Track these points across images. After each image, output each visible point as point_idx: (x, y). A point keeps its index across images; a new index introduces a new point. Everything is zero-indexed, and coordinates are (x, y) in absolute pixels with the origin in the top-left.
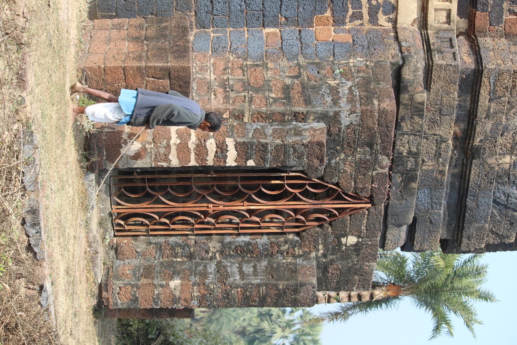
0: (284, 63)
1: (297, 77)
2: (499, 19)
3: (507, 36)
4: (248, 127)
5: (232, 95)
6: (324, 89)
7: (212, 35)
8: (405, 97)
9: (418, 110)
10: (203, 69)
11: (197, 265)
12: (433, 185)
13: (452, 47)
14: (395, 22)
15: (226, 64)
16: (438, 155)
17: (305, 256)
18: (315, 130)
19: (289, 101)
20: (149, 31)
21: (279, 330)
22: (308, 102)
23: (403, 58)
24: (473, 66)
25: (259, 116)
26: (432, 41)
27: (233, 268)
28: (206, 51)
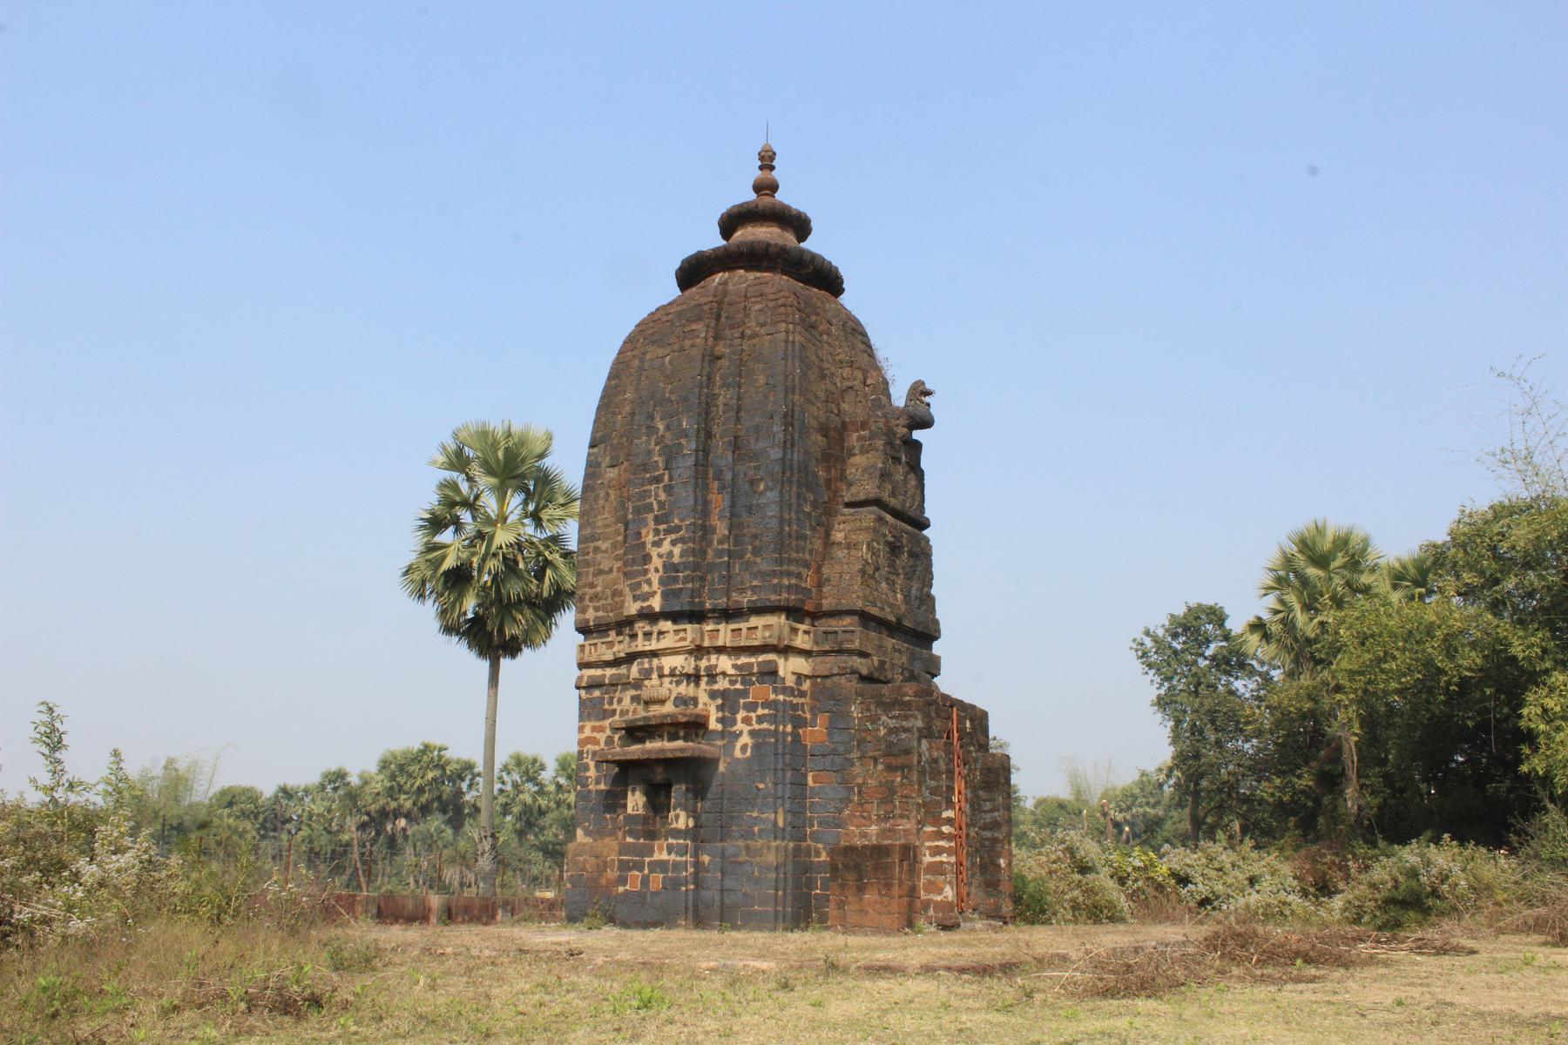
0: (857, 769)
1: (875, 760)
2: (809, 591)
3: (820, 585)
5: (898, 812)
6: (893, 738)
8: (876, 675)
9: (882, 663)
10: (864, 835)
11: (982, 845)
12: (912, 657)
16: (900, 651)
17: (976, 760)
21: (521, 796)
22: (907, 752)
23: (853, 672)
25: (920, 790)
27: (988, 818)
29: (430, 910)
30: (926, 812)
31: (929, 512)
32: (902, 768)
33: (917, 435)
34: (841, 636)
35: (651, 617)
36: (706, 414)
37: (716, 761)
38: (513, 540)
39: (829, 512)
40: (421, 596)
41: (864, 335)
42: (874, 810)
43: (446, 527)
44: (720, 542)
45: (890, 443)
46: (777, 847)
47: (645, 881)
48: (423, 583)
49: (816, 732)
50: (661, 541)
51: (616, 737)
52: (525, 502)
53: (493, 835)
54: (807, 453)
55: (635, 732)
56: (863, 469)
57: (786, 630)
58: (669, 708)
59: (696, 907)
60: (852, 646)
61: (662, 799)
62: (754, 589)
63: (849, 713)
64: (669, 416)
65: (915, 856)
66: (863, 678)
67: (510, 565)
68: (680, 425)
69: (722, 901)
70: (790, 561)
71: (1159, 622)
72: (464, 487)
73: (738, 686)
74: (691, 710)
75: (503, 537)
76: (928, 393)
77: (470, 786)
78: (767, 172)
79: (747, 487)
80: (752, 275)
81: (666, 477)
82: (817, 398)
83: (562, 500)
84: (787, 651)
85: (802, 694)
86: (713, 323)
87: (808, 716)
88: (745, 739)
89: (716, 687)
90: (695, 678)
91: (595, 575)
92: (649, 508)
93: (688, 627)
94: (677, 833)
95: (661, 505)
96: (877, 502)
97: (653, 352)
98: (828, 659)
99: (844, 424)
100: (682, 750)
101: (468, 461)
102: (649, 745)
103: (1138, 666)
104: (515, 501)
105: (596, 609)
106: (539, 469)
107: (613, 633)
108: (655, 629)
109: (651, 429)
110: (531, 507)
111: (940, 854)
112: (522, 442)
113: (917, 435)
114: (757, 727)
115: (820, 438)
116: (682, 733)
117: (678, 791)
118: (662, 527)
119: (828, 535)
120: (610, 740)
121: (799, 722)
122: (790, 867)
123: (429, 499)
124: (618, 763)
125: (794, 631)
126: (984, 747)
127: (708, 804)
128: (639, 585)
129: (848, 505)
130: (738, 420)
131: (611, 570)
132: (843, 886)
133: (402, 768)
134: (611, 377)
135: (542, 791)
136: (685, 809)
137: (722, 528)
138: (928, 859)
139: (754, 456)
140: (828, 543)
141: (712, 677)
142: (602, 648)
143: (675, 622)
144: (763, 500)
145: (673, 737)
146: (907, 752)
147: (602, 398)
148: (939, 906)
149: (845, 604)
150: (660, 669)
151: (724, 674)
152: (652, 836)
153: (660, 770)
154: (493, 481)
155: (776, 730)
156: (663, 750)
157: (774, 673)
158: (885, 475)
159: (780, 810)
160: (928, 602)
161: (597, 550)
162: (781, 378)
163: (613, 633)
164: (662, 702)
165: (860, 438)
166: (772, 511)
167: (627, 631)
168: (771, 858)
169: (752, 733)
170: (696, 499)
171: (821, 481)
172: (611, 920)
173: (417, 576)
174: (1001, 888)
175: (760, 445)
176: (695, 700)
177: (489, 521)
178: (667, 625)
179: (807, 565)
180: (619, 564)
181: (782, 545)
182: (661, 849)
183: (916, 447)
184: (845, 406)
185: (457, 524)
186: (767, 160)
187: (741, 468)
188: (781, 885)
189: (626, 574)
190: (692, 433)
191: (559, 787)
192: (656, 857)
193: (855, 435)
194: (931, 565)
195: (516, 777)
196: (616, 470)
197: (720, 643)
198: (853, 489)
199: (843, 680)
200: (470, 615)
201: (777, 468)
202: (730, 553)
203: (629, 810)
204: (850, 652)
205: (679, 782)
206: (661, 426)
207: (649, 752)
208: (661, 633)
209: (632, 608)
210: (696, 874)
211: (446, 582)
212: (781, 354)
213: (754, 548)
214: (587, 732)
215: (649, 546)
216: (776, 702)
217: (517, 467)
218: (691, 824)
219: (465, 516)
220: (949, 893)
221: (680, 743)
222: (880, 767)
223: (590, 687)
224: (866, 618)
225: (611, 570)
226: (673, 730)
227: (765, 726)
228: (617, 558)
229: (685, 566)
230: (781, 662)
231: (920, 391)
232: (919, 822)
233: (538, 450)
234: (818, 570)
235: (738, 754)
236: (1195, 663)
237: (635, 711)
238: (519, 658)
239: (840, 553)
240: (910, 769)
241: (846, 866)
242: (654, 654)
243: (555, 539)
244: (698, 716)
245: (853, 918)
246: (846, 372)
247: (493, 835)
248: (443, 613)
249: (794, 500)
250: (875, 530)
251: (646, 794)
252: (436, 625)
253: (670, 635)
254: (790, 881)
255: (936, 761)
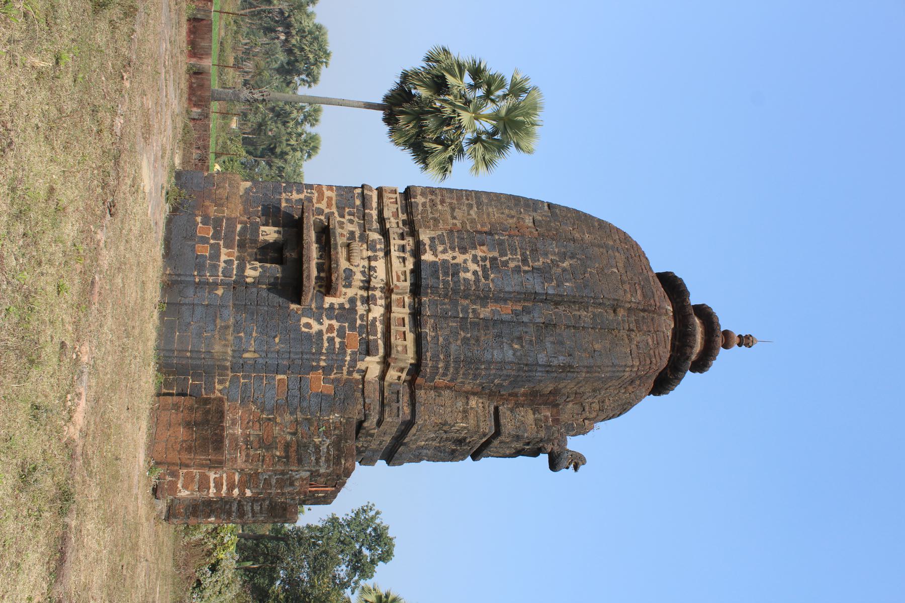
0: (288, 417)
1: (294, 434)
3: (436, 388)
4: (261, 477)
5: (252, 452)
6: (312, 449)
7: (242, 381)
9: (372, 435)
10: (234, 423)
12: (374, 451)
13: (398, 402)
14: (364, 377)
15: (249, 416)
16: (380, 444)
18: (302, 479)
19: (288, 461)
20: (198, 415)
22: (300, 461)
23: (365, 415)
24: (409, 418)
26: (386, 394)
27: (248, 508)
28: (237, 401)
29: (201, 58)
30: (251, 475)
31: (486, 462)
32: (287, 457)
33: (544, 458)
34: (395, 405)
35: (417, 252)
36: (573, 301)
37: (299, 303)
38: (463, 124)
39: (491, 395)
40: (428, 59)
41: (619, 416)
42: (254, 432)
43: (474, 79)
44: (474, 311)
45: (541, 440)
46: (226, 353)
47: (204, 240)
48: (437, 61)
49: (319, 383)
50: (477, 263)
51: (322, 218)
52: (487, 133)
53: (264, 100)
54: (540, 381)
55: (325, 234)
56: (523, 420)
57: (402, 365)
58: (344, 264)
59: (181, 282)
60: (386, 416)
61: (271, 254)
62: (436, 338)
63: (333, 411)
64: (573, 271)
65: (215, 467)
66: (360, 424)
67: (448, 121)
68: (567, 281)
69: (186, 304)
70: (457, 370)
71: (383, 520)
72: (500, 93)
73: (359, 322)
74: (341, 283)
75: (465, 117)
76: (576, 468)
77: (303, 80)
78: (737, 340)
79: (517, 334)
80: (670, 334)
81: (526, 268)
82: (579, 388)
83: (487, 157)
84: (386, 364)
85: (350, 373)
86: (641, 307)
87: (332, 376)
88: (316, 327)
89: (359, 303)
90: (367, 285)
91: (450, 204)
92: (503, 254)
93: (408, 284)
94: (241, 268)
95: (505, 264)
96: (498, 433)
97: (620, 258)
98: (377, 394)
99: (558, 405)
100: (309, 276)
101: (517, 96)
102: (314, 247)
103: (357, 507)
104: (488, 126)
105: (424, 205)
106: (508, 143)
107: (404, 217)
108: (407, 255)
109: (563, 256)
110: (484, 137)
111: (216, 487)
112: (528, 134)
113: (544, 458)
114: (325, 337)
115: (550, 389)
116: (322, 275)
117: (276, 270)
118: (488, 263)
119: (474, 394)
120: (320, 212)
121: (327, 370)
122: (210, 362)
123: (492, 68)
124: (301, 219)
125: (401, 370)
126: (303, 502)
127: (264, 294)
128: (443, 243)
129: (496, 409)
130: (568, 327)
131: (454, 218)
132: (191, 409)
133: (316, 38)
134: (601, 223)
135: (298, 124)
136: (260, 276)
137: (485, 312)
138: (212, 476)
139: (540, 340)
140: (467, 395)
141: (367, 300)
142: (393, 208)
143: (412, 271)
144: (506, 347)
145: (320, 268)
146: (300, 461)
147: (585, 215)
148: (173, 487)
149: (420, 409)
150: (375, 258)
151: (369, 310)
152: (242, 246)
153: (294, 255)
154: (503, 112)
155: (321, 354)
156: (309, 261)
157: (368, 353)
158: (518, 438)
159: (256, 355)
160: (418, 458)
161: (470, 206)
162: (599, 363)
163: (404, 217)
164: (349, 259)
165: (546, 417)
166: (497, 355)
167: (406, 229)
168: (217, 348)
169: (320, 333)
170: (510, 293)
171: (516, 390)
172: (175, 210)
173: (442, 57)
174: (191, 518)
175: (548, 345)
176: (349, 286)
177: (477, 108)
178: (410, 265)
179: (452, 380)
180: (459, 225)
181: (470, 363)
182: (229, 255)
183: (535, 453)
184: (570, 405)
185: (473, 87)
186: (745, 341)
187: (531, 329)
188: (195, 355)
189: (451, 231)
190: (561, 291)
191: (300, 135)
192: (224, 251)
193: (549, 414)
194: (443, 460)
195: (307, 109)
196: (531, 224)
197: (394, 308)
198: (509, 412)
199: (360, 407)
200: (413, 91)
201: (531, 360)
202: (464, 319)
203: (262, 228)
204: (382, 413)
205: (283, 271)
206: (565, 264)
207: (309, 249)
208: (404, 259)
209: (425, 236)
210: (208, 283)
211: (437, 77)
212: (616, 362)
213: (468, 339)
214: (328, 193)
215: (473, 252)
216: (345, 352)
217: (511, 129)
218: (249, 280)
219: (480, 92)
220: (184, 493)
221: (314, 273)
222: (289, 438)
223: (363, 196)
224: (408, 425)
225: (454, 218)
226: (325, 267)
227: (326, 344)
228: (463, 223)
229: (457, 283)
230: (377, 359)
231: (577, 462)
232: (242, 470)
233: (522, 144)
234: (448, 387)
235: (304, 320)
236: (357, 541)
237: (342, 235)
238: (383, 123)
239: (460, 404)
240: (287, 464)
241: (207, 412)
242: (387, 253)
243: (461, 151)
244: (336, 289)
245: (165, 416)
246: (596, 406)
247: (264, 100)
248: (417, 74)
249: (505, 372)
250: (476, 432)
251: (275, 242)
252: (409, 68)
253: (402, 267)
254: (198, 362)
255: (292, 484)
